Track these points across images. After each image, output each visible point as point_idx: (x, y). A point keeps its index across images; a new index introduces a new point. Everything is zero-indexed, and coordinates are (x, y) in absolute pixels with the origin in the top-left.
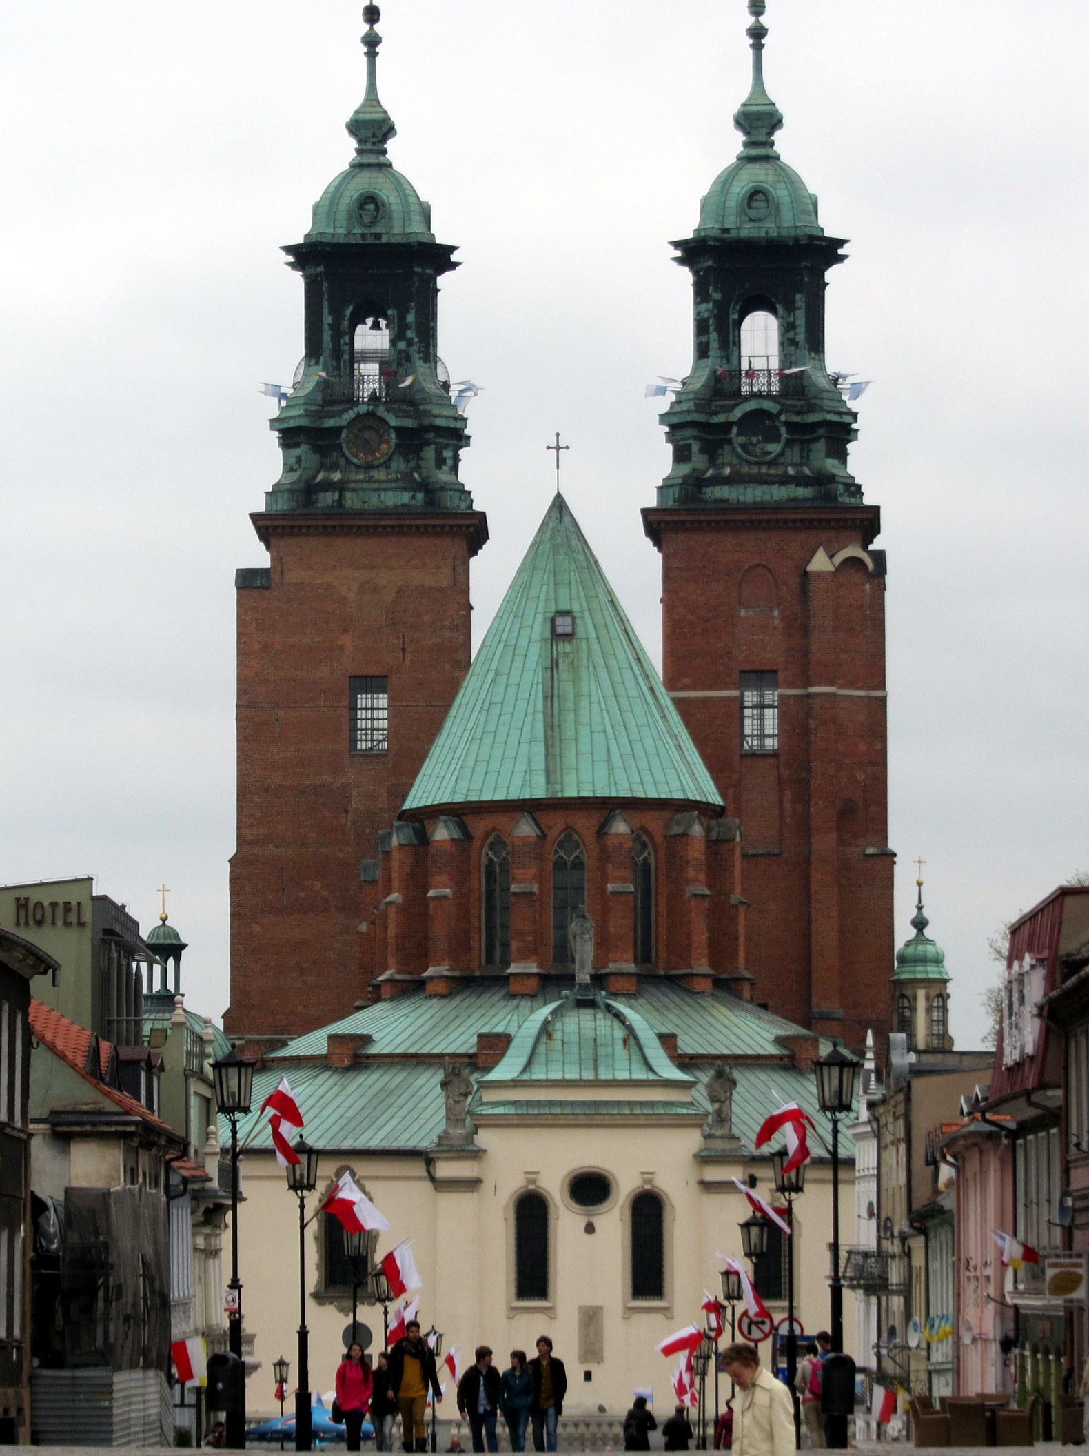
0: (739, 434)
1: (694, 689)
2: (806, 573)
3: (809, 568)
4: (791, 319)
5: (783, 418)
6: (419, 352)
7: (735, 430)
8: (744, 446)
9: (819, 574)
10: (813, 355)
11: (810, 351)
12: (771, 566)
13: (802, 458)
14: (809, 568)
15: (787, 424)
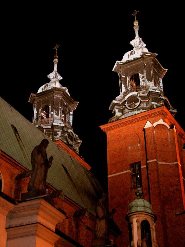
0: (128, 103)
1: (116, 172)
2: (144, 130)
3: (145, 128)
4: (143, 75)
5: (138, 95)
6: (55, 113)
7: (127, 102)
8: (129, 106)
9: (148, 128)
10: (149, 82)
11: (148, 81)
12: (137, 133)
13: (147, 106)
14: (145, 128)
15: (140, 96)
